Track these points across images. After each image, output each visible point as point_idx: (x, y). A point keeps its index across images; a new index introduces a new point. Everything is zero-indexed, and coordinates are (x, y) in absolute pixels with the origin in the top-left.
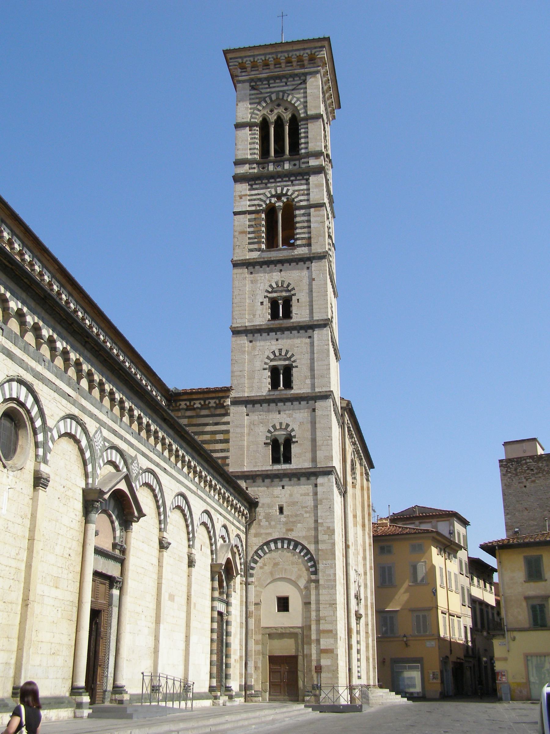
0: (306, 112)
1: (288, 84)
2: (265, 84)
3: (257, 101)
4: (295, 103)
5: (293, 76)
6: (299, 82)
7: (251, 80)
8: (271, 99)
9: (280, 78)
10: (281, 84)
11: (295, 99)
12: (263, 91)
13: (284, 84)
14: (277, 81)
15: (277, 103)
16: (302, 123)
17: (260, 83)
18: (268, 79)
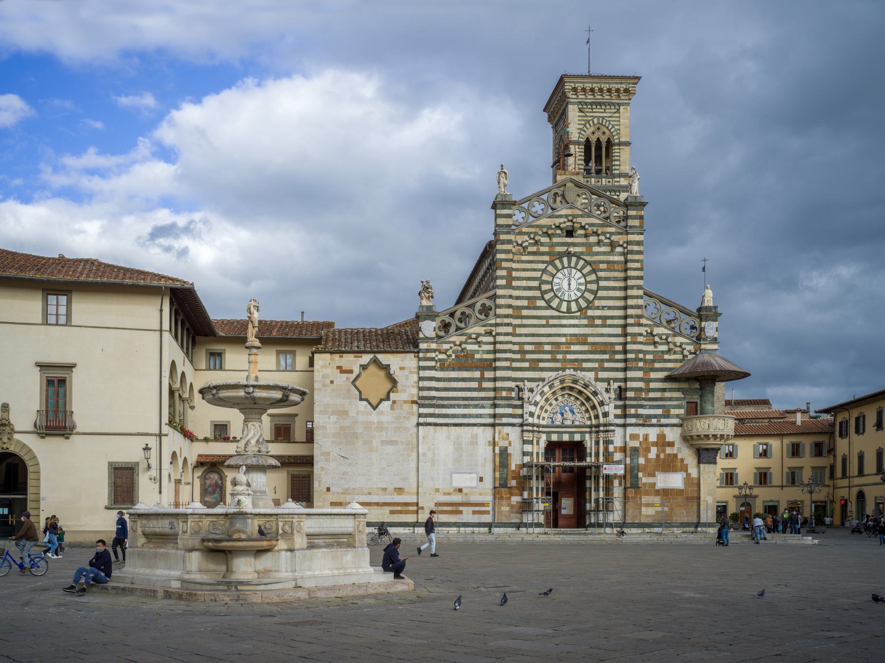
0: (619, 138)
1: (607, 111)
2: (589, 108)
3: (583, 122)
4: (611, 129)
5: (610, 104)
6: (615, 111)
7: (580, 103)
8: (593, 122)
9: (600, 104)
10: (601, 110)
11: (610, 127)
12: (588, 114)
13: (603, 111)
14: (598, 107)
15: (597, 126)
16: (616, 147)
17: (585, 107)
18: (591, 104)
